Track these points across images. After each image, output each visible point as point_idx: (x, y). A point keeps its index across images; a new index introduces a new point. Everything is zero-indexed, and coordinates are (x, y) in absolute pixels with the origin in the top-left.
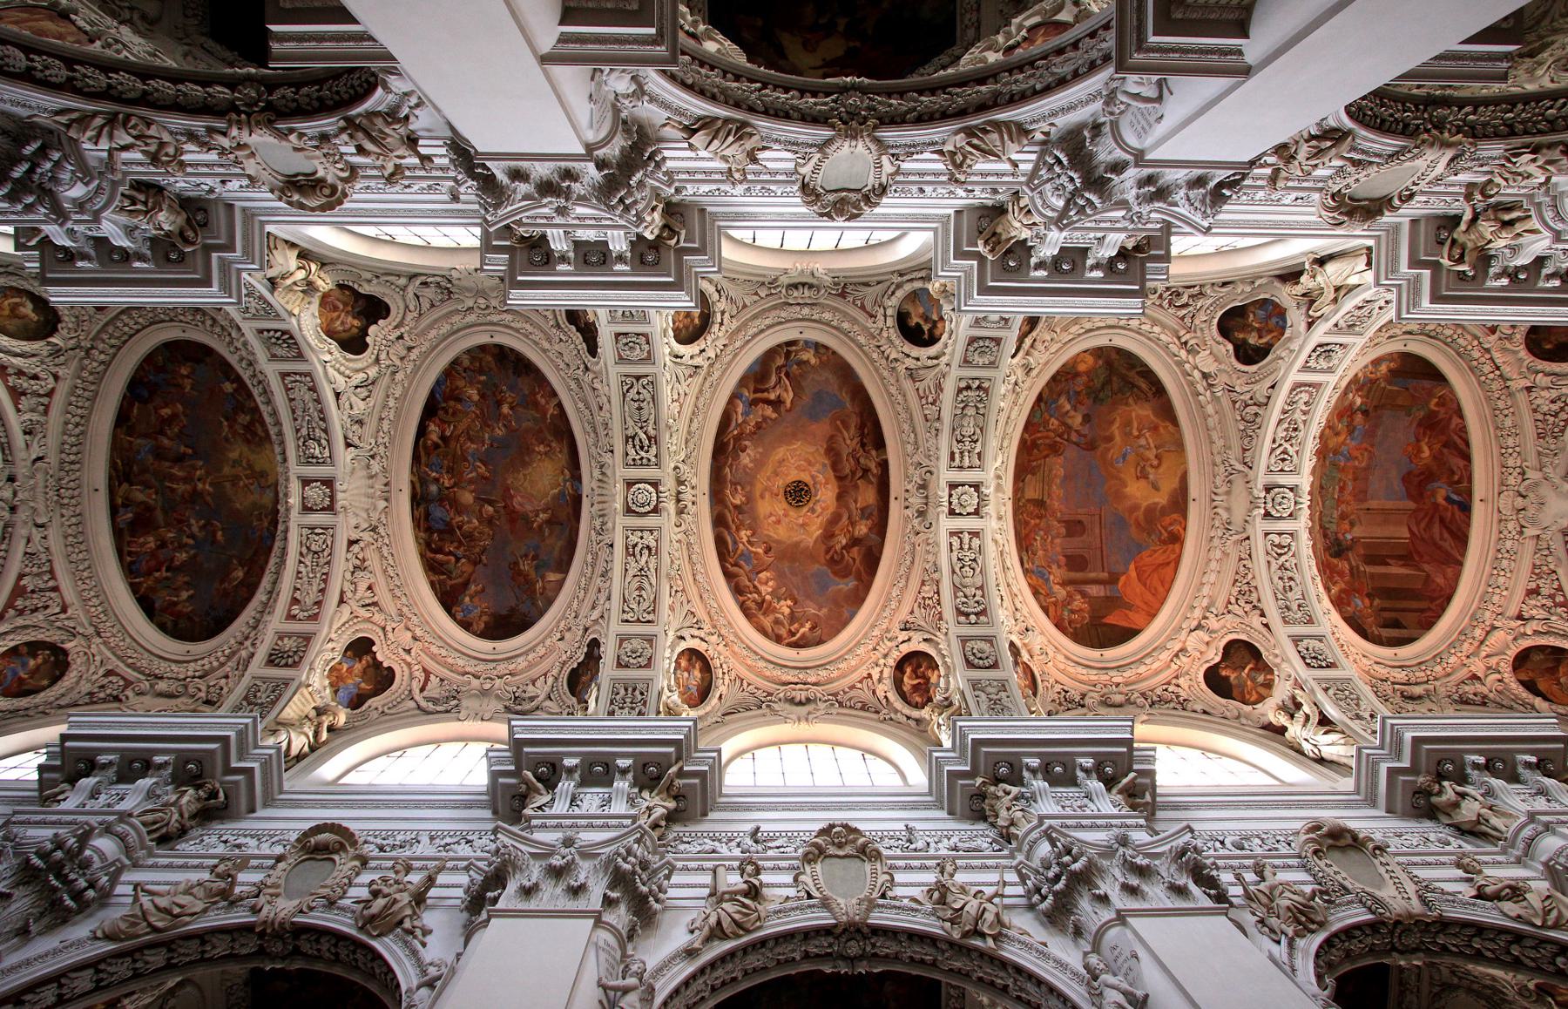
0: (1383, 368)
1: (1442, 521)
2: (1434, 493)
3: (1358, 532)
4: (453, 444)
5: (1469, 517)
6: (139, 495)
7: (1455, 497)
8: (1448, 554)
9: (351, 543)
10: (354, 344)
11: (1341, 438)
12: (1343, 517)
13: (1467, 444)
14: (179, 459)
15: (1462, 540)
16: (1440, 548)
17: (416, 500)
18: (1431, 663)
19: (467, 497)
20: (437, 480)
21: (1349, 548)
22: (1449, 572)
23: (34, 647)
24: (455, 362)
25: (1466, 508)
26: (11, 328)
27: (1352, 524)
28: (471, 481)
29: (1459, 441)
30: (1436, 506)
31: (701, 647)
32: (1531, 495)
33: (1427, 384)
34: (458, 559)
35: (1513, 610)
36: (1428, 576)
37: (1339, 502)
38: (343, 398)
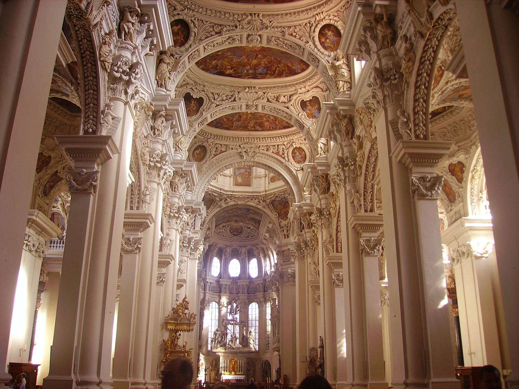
4: (234, 66)
6: (252, 125)
9: (268, 101)
10: (200, 102)
14: (240, 117)
17: (255, 77)
19: (255, 62)
20: (247, 70)
23: (293, 152)
24: (203, 69)
26: (203, 154)
28: (248, 60)
31: (320, 26)
34: (278, 67)
38: (218, 103)
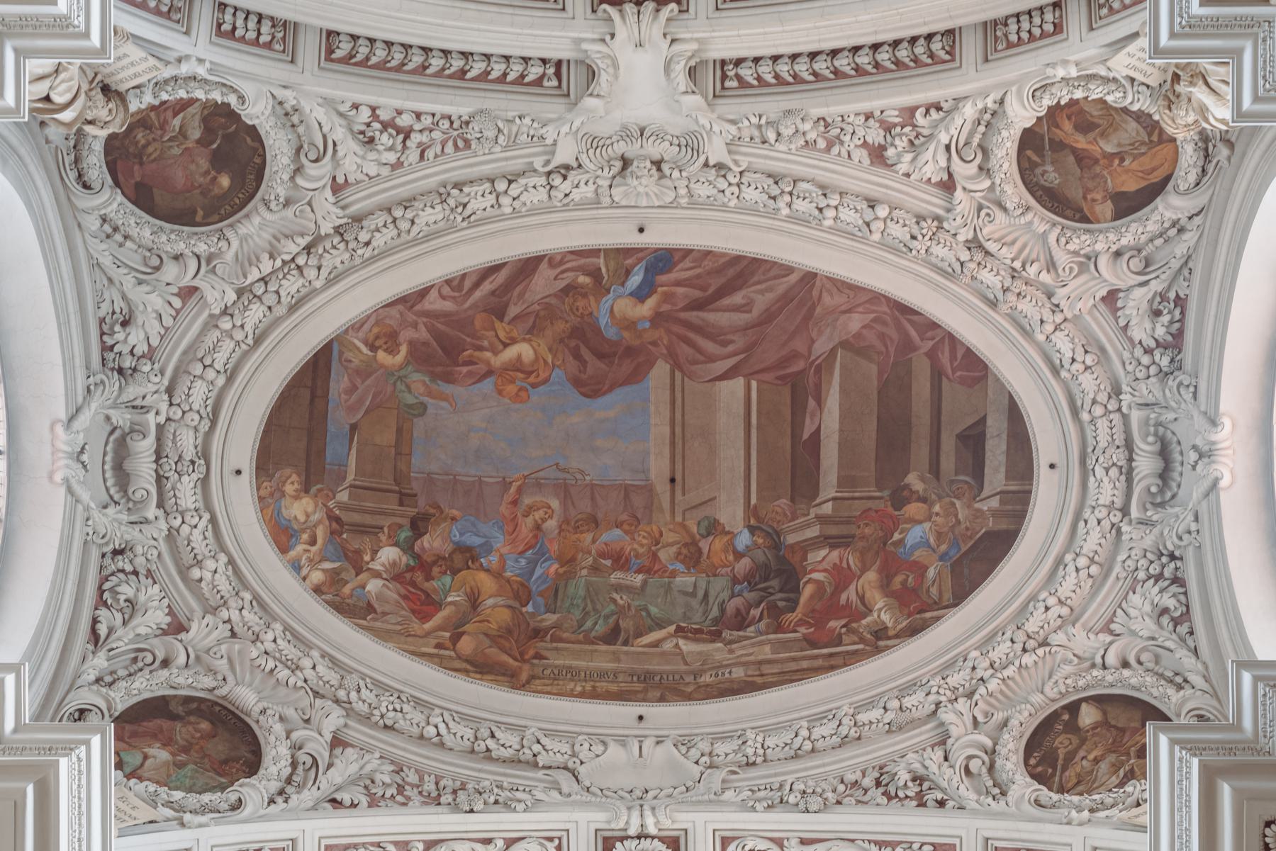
0: (299, 509)
1: (698, 305)
2: (630, 325)
3: (731, 514)
5: (687, 252)
7: (636, 280)
8: (786, 298)
11: (486, 582)
12: (692, 557)
13: (495, 269)
15: (743, 270)
16: (768, 317)
18: (1076, 390)
21: (775, 540)
22: (827, 299)
25: (663, 260)
27: (713, 527)
29: (487, 287)
30: (658, 319)
32: (620, 148)
33: (338, 384)
35: (932, 202)
36: (844, 344)
37: (651, 567)
